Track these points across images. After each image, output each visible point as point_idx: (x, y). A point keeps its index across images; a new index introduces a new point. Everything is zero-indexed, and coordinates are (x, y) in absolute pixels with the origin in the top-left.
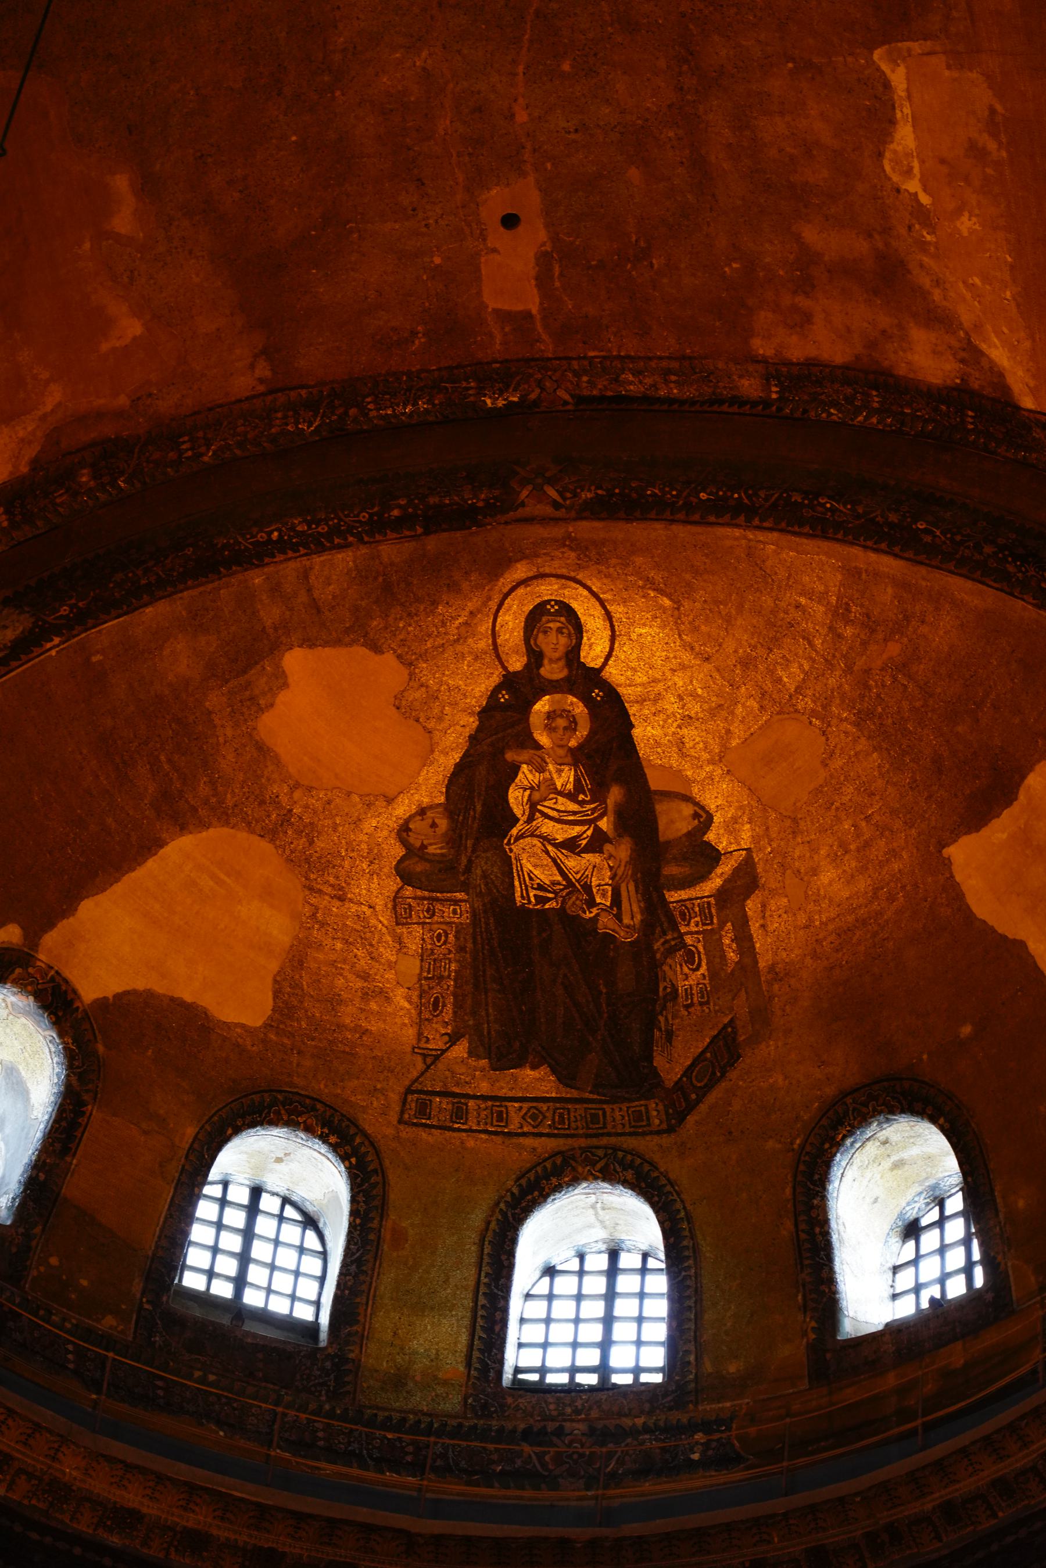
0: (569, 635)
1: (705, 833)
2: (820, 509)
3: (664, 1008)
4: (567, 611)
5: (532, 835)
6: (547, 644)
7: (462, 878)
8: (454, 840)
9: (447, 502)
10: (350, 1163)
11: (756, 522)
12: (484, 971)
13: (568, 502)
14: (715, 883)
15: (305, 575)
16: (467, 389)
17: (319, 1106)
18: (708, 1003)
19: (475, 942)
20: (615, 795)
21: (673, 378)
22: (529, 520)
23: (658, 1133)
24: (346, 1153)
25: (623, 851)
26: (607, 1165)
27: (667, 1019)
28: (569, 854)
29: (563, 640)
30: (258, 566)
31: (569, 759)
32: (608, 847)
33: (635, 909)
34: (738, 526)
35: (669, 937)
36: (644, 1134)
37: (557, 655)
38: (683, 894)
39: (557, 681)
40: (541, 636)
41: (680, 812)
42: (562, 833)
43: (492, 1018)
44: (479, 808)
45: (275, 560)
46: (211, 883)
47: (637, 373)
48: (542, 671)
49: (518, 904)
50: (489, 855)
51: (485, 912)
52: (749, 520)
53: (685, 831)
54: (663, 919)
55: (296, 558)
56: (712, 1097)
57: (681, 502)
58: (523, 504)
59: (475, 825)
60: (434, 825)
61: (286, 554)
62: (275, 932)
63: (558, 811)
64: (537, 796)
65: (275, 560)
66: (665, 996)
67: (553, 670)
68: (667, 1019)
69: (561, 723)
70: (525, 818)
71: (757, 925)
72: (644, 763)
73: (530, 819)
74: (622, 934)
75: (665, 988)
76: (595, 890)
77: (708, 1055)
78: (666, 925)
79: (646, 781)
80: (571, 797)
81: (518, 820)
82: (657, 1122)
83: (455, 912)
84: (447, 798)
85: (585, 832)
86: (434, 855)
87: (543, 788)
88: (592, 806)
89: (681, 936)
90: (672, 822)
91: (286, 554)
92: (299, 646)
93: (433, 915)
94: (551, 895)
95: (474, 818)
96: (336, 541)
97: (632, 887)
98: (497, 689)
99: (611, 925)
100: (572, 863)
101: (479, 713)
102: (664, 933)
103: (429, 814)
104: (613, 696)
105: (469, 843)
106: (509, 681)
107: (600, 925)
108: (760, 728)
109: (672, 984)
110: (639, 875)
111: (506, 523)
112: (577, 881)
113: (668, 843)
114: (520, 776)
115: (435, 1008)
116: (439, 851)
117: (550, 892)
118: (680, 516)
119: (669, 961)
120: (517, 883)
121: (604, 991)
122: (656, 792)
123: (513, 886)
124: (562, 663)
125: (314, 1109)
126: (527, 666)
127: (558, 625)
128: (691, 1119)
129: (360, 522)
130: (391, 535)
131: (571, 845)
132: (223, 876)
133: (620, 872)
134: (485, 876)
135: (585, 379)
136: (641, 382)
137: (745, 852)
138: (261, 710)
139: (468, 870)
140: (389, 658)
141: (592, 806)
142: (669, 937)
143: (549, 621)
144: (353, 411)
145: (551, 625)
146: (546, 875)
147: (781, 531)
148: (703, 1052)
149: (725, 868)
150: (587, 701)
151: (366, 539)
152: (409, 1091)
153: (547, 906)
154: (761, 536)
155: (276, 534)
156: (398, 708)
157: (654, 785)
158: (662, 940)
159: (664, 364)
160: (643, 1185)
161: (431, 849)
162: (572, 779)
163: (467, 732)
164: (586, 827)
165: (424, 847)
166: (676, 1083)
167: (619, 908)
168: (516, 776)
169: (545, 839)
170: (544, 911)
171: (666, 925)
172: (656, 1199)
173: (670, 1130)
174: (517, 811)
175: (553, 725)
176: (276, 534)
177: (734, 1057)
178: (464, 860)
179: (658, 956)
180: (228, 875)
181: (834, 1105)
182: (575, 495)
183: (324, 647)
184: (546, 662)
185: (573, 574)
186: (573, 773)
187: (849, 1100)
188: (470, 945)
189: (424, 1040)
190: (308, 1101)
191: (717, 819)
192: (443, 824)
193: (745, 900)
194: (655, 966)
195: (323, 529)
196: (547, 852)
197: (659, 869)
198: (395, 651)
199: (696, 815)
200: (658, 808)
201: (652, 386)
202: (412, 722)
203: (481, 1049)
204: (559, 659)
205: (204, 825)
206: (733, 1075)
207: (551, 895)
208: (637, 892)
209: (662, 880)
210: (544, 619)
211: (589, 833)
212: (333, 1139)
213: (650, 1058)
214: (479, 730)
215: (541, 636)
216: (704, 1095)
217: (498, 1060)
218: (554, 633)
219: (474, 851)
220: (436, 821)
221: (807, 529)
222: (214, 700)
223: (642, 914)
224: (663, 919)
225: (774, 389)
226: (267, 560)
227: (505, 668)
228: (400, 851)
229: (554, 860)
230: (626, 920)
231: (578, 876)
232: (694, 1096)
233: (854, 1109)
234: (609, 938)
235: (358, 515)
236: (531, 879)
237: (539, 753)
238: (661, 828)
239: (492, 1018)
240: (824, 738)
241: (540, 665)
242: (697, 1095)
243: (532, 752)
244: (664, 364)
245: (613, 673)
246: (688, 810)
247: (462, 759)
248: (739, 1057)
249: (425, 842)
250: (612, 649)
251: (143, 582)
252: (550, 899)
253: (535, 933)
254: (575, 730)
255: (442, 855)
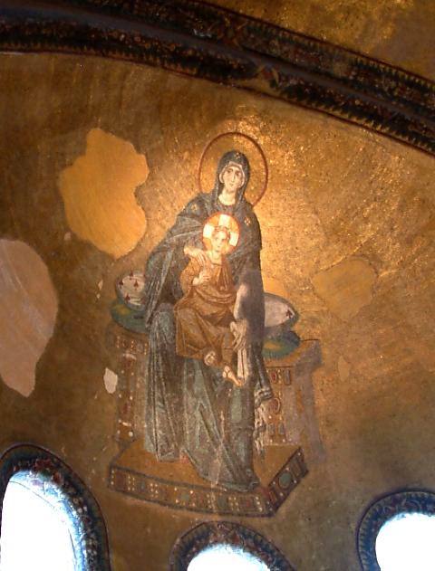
0: (241, 178)
1: (292, 326)
2: (419, 127)
3: (258, 435)
4: (245, 161)
5: (190, 307)
6: (228, 180)
7: (147, 326)
8: (146, 299)
9: (219, 57)
10: (83, 511)
11: (379, 128)
12: (154, 393)
13: (281, 84)
14: (295, 360)
15: (124, 76)
16: (188, 18)
17: (62, 465)
18: (285, 436)
19: (149, 370)
20: (242, 291)
21: (300, 51)
22: (250, 90)
23: (263, 516)
24: (80, 502)
25: (239, 329)
26: (235, 535)
27: (260, 443)
28: (209, 324)
29: (237, 180)
30: (104, 56)
31: (219, 262)
32: (233, 324)
33: (245, 368)
34: (367, 128)
35: (263, 390)
36: (254, 516)
37: (232, 188)
38: (275, 363)
39: (227, 206)
40: (226, 173)
41: (279, 309)
42: (209, 310)
43: (157, 425)
44: (163, 280)
45: (114, 56)
46: (11, 281)
47: (283, 42)
48: (221, 197)
49: (177, 351)
50: (164, 313)
51: (157, 352)
52: (375, 125)
53: (280, 322)
54: (262, 377)
55: (126, 60)
56: (294, 495)
57: (343, 103)
58: (256, 76)
59: (160, 291)
60: (136, 285)
61: (121, 54)
62: (40, 331)
63: (207, 294)
64: (196, 281)
65: (114, 56)
66: (258, 429)
67: (226, 199)
68: (260, 443)
69: (222, 235)
70: (186, 295)
71: (319, 388)
72: (263, 274)
73: (191, 296)
74: (237, 383)
75: (258, 423)
76: (223, 351)
77: (287, 469)
78: (263, 381)
79: (262, 286)
80: (217, 286)
81: (183, 295)
82: (261, 509)
83: (140, 348)
84: (147, 269)
85: (221, 312)
86: (134, 306)
87: (201, 276)
88: (228, 295)
89: (271, 390)
90: (274, 315)
91: (121, 54)
92: (101, 128)
93: (127, 347)
94: (196, 350)
95: (159, 286)
96: (151, 58)
97: (245, 353)
98: (192, 201)
99: (231, 375)
100: (212, 330)
101: (179, 215)
102: (261, 386)
103: (135, 277)
104: (256, 227)
105: (154, 303)
106: (199, 200)
107: (224, 375)
108: (338, 264)
109: (263, 422)
110: (250, 346)
111: (239, 88)
112: (213, 343)
113: (269, 328)
114: (190, 264)
115: (126, 412)
116: (136, 304)
117: (195, 347)
118: (337, 113)
119: (262, 405)
120: (177, 337)
121: (223, 418)
122: (269, 295)
123: (174, 337)
124: (234, 194)
125: (59, 466)
126: (213, 191)
127: (237, 169)
128: (283, 510)
129: (169, 50)
130: (180, 68)
131: (211, 319)
132: (17, 278)
133: (238, 342)
134: (159, 328)
135: (252, 36)
136: (281, 48)
137: (315, 342)
138: (64, 166)
139: (150, 322)
140: (143, 156)
141: (228, 295)
142: (263, 390)
143: (232, 165)
144: (126, 5)
145: (233, 168)
146: (195, 333)
147: (391, 137)
148: (284, 467)
149: (303, 349)
150: (241, 224)
151: (166, 65)
152: (111, 467)
153: (193, 356)
154: (379, 138)
155: (123, 36)
156: (136, 196)
157: (265, 290)
158: (260, 391)
159: (301, 40)
160: (260, 549)
161: (132, 301)
162: (218, 275)
163: (169, 226)
164: (221, 309)
165: (128, 298)
166: (270, 485)
167: (236, 365)
168: (187, 263)
169: (198, 312)
170: (192, 359)
171: (263, 381)
172: (270, 559)
173: (270, 515)
174: (184, 287)
175: (217, 236)
176: (123, 36)
177: (305, 473)
178: (149, 315)
179: (256, 401)
180: (21, 279)
181: (372, 505)
182: (287, 80)
183: (113, 134)
184: (224, 191)
185: (256, 138)
186: (219, 271)
187: (381, 502)
188: (147, 373)
189: (119, 432)
190: (55, 460)
191: (303, 316)
192: (142, 285)
193: (311, 372)
194: (253, 407)
195: (147, 46)
196: (197, 321)
197: (262, 344)
198: (146, 155)
199: (289, 313)
200: (266, 304)
201: (286, 52)
202: (140, 208)
203: (152, 445)
204: (232, 192)
205: (15, 237)
206: (303, 481)
207: (196, 350)
208: (248, 354)
209: (263, 352)
210: (230, 163)
211: (223, 313)
212: (71, 491)
213: (251, 467)
214: (174, 227)
215: (226, 173)
216: (288, 494)
217: (162, 455)
218: (234, 173)
219: (155, 309)
220: (139, 283)
221: (406, 139)
222: (43, 146)
223: (249, 371)
224: (262, 377)
225: (353, 73)
226: (110, 53)
227: (200, 189)
228: (115, 297)
229: (201, 328)
230: (240, 374)
231: (214, 340)
232: (282, 494)
233: (386, 509)
234: (229, 383)
235: (169, 45)
236: (186, 337)
237: (203, 252)
238: (266, 317)
239: (157, 425)
240: (375, 275)
241: (220, 192)
242: (284, 494)
243: (200, 250)
244: (301, 40)
245: (256, 210)
246: (284, 309)
247: (160, 244)
248: (307, 472)
249: (130, 295)
250: (263, 193)
251: (44, 32)
252: (195, 352)
253: (185, 373)
254: (228, 241)
255: (138, 306)
